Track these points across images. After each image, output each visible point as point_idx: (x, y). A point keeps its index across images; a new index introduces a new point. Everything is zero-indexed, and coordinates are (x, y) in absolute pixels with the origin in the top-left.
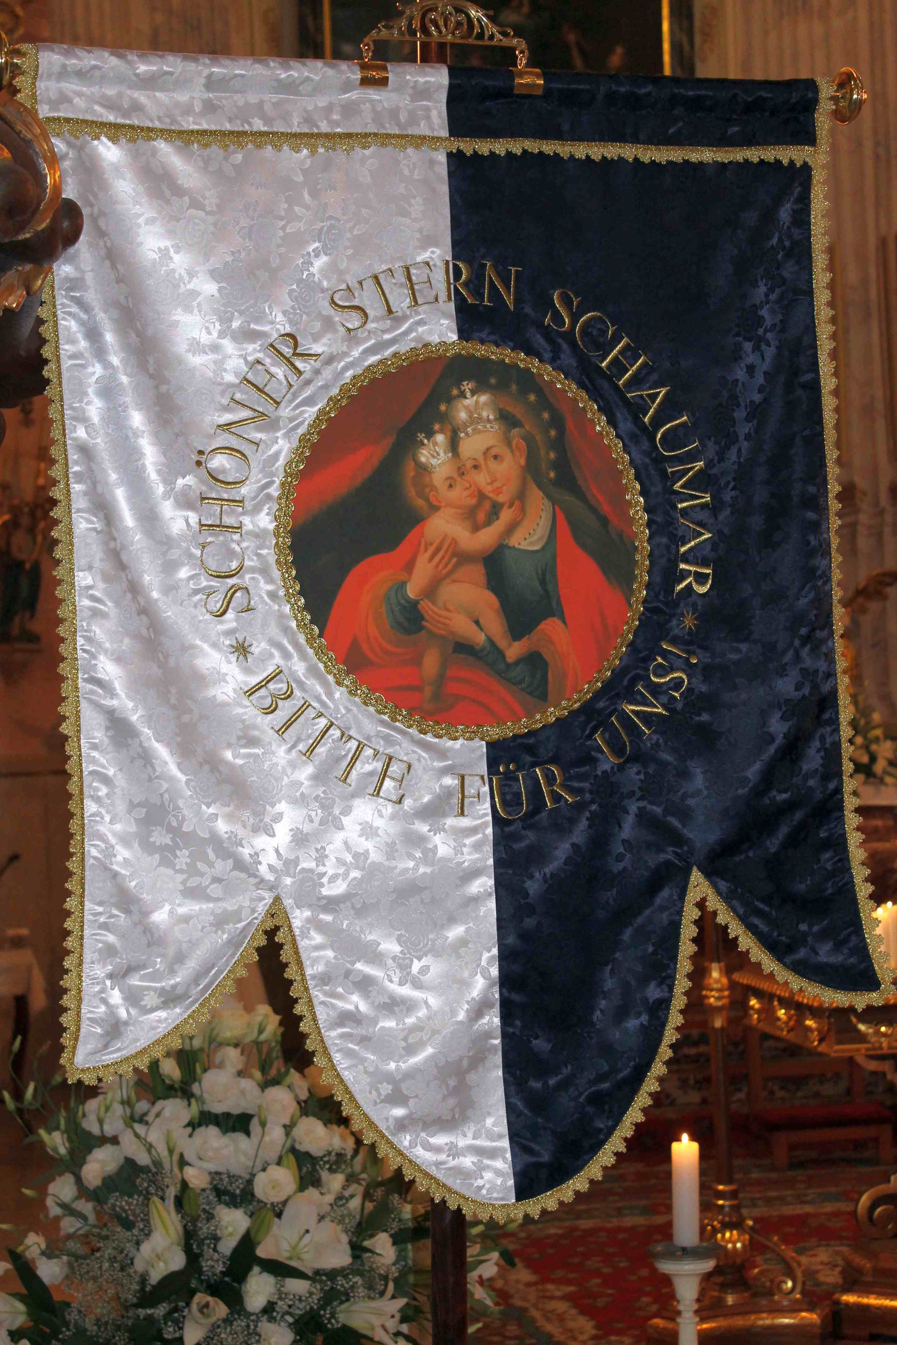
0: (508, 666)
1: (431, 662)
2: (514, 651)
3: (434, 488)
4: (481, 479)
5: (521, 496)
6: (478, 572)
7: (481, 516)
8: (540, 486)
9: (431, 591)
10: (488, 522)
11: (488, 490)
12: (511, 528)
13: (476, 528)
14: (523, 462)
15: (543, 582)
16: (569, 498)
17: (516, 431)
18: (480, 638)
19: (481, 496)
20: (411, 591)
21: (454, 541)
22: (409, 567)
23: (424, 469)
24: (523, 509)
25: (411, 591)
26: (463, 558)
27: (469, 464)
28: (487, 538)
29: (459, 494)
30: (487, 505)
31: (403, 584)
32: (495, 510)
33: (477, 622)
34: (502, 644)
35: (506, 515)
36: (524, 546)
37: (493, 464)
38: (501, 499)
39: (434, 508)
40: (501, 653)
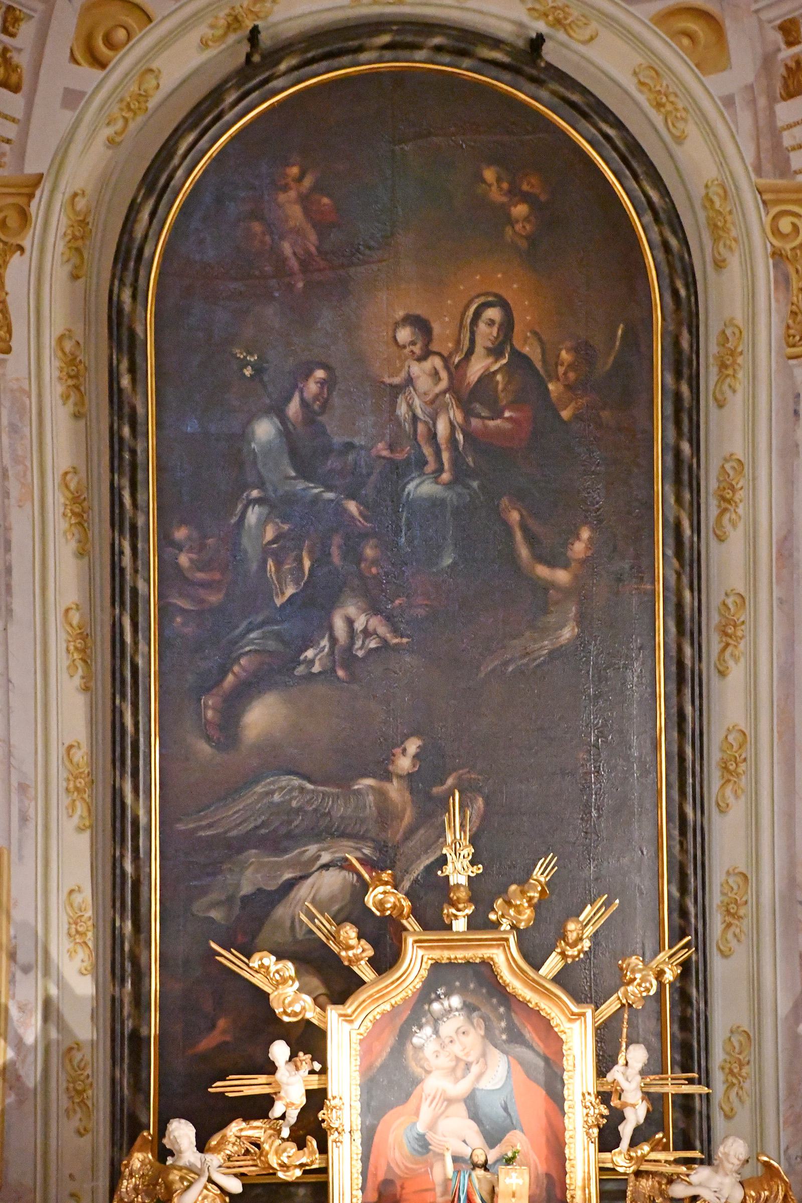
28: (462, 1088)
29: (445, 1061)
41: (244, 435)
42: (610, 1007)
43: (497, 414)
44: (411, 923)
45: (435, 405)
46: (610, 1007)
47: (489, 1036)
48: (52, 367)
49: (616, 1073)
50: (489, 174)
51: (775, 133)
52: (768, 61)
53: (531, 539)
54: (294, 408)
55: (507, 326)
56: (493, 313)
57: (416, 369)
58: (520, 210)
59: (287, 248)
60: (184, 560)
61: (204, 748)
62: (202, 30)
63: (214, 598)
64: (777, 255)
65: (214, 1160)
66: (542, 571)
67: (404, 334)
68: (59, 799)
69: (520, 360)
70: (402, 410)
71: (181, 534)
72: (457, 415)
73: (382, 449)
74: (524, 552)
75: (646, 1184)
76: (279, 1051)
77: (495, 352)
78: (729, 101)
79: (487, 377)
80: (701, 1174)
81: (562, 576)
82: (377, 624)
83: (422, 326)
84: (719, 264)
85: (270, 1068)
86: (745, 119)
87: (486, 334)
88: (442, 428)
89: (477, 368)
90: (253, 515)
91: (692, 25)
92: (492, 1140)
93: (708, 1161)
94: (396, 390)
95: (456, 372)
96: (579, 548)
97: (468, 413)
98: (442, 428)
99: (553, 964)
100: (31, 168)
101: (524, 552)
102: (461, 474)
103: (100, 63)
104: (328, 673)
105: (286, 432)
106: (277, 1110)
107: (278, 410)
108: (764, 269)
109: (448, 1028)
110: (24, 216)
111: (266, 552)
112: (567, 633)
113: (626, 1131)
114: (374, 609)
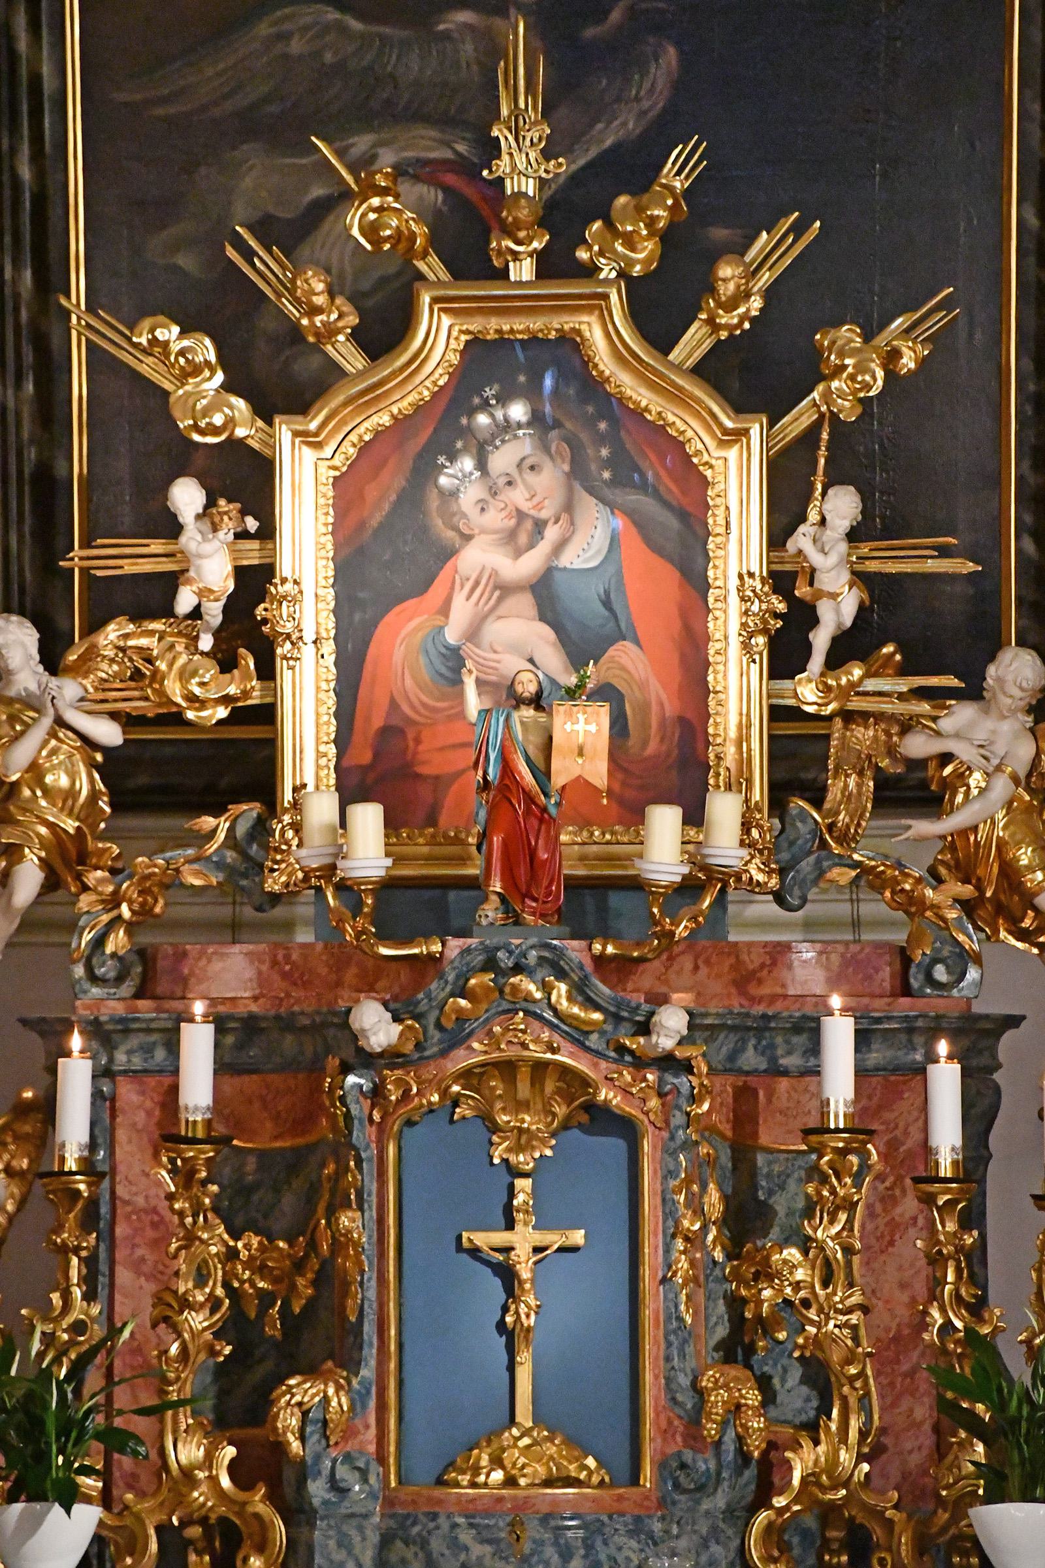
3: (464, 515)
4: (518, 497)
5: (569, 507)
6: (525, 603)
7: (523, 539)
8: (591, 491)
9: (473, 634)
10: (531, 546)
11: (525, 506)
12: (559, 547)
13: (518, 553)
14: (566, 467)
15: (607, 603)
16: (634, 498)
17: (554, 434)
19: (521, 515)
21: (494, 573)
22: (445, 610)
25: (452, 636)
26: (505, 590)
27: (502, 481)
28: (530, 564)
29: (496, 518)
30: (528, 525)
31: (441, 629)
32: (540, 527)
35: (552, 533)
36: (578, 564)
38: (544, 514)
39: (467, 538)
44: (432, 267)
47: (578, 473)
49: (802, 540)
65: (69, 689)
75: (863, 735)
80: (961, 715)
85: (172, 528)
92: (578, 657)
93: (974, 692)
106: (185, 601)
109: (502, 459)
113: (821, 639)
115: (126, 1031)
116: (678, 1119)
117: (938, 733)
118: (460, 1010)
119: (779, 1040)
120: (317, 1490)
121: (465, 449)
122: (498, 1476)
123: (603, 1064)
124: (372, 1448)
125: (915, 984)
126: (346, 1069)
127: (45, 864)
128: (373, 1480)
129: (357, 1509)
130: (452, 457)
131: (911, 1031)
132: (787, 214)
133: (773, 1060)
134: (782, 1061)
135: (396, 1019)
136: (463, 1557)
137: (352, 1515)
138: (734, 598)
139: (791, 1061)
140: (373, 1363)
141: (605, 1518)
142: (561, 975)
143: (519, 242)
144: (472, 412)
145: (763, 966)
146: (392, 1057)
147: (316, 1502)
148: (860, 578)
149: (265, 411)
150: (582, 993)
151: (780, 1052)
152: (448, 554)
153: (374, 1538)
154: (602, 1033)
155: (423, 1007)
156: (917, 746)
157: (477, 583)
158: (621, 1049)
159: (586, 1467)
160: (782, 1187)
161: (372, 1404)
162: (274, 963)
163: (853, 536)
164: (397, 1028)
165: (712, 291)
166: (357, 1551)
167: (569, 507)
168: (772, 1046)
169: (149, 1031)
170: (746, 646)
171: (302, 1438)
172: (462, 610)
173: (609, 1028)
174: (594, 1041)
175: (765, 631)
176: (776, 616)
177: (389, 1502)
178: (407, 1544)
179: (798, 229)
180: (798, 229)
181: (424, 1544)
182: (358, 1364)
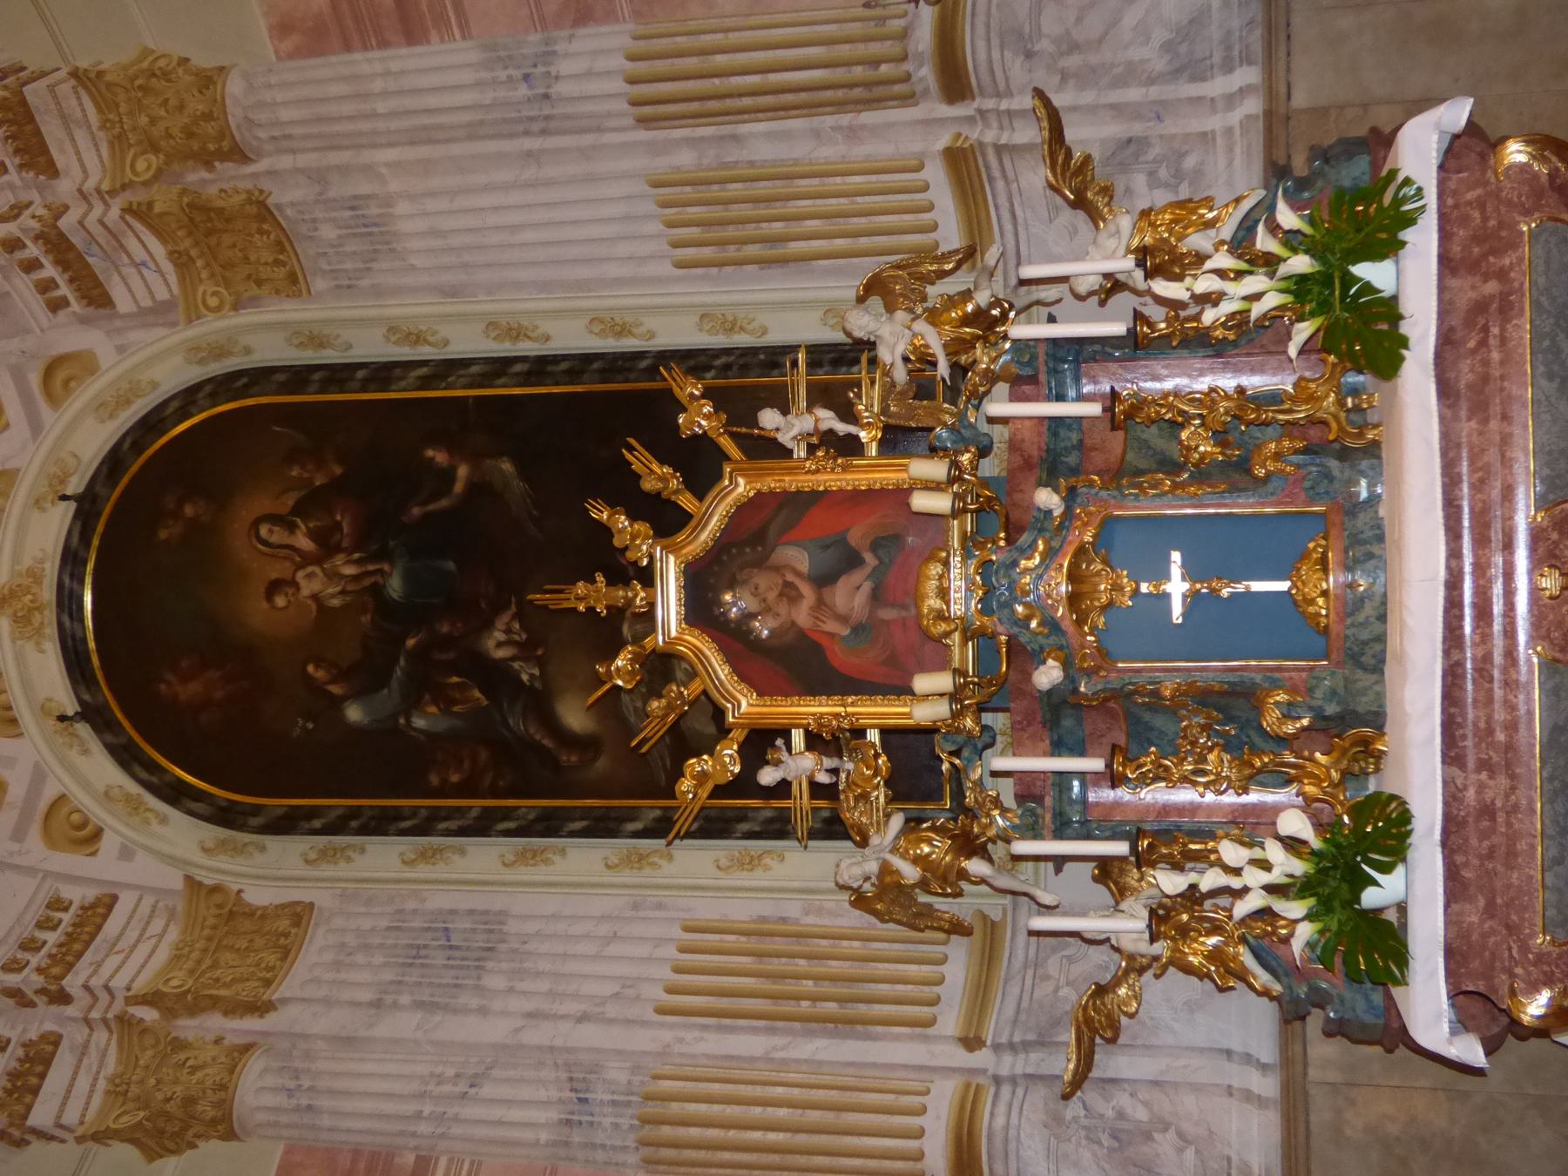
0: (881, 562)
1: (887, 614)
2: (870, 559)
3: (781, 625)
4: (772, 596)
5: (777, 569)
6: (826, 592)
8: (768, 557)
9: (843, 619)
10: (796, 588)
12: (798, 574)
13: (800, 596)
14: (756, 571)
15: (828, 547)
17: (738, 577)
18: (867, 587)
19: (781, 595)
20: (846, 632)
21: (812, 609)
22: (831, 635)
23: (772, 632)
24: (786, 566)
25: (846, 632)
26: (820, 604)
27: (763, 605)
28: (807, 590)
29: (783, 609)
31: (843, 638)
32: (788, 584)
33: (858, 588)
34: (868, 570)
35: (790, 577)
37: (761, 590)
38: (780, 581)
39: (793, 623)
40: (874, 569)
41: (356, 730)
42: (727, 443)
43: (338, 526)
45: (333, 576)
46: (727, 443)
47: (760, 563)
48: (327, 871)
50: (163, 534)
51: (142, 312)
52: (83, 321)
53: (435, 496)
54: (336, 689)
55: (275, 519)
56: (264, 530)
57: (306, 591)
58: (189, 510)
59: (219, 694)
60: (455, 778)
61: (602, 764)
62: (74, 755)
63: (484, 755)
64: (236, 307)
66: (459, 487)
67: (280, 601)
68: (646, 875)
69: (300, 510)
70: (336, 602)
71: (434, 780)
72: (339, 560)
73: (366, 619)
74: (444, 503)
76: (768, 776)
77: (292, 528)
78: (121, 349)
79: (313, 535)
80: (884, 354)
81: (463, 471)
82: (502, 621)
83: (274, 587)
84: (248, 351)
86: (134, 336)
87: (278, 536)
88: (349, 570)
89: (304, 542)
90: (419, 722)
91: (60, 376)
93: (871, 345)
94: (322, 608)
95: (307, 560)
96: (439, 457)
97: (338, 549)
98: (349, 570)
99: (687, 501)
100: (178, 883)
101: (444, 503)
102: (383, 555)
103: (98, 834)
104: (541, 663)
105: (356, 695)
106: (823, 778)
107: (337, 703)
108: (248, 317)
110: (216, 889)
111: (446, 711)
112: (507, 466)
113: (842, 428)
114: (488, 625)
115: (1061, 814)
116: (1104, 494)
117: (892, 365)
118: (1039, 625)
119: (1062, 445)
120: (1331, 709)
121: (747, 625)
122: (1321, 601)
123: (1070, 538)
124: (1304, 675)
125: (1027, 371)
126: (1075, 691)
127: (969, 857)
128: (1324, 675)
129: (1341, 684)
130: (750, 631)
131: (1056, 371)
132: (623, 456)
133: (1073, 447)
134: (1075, 442)
135: (1044, 662)
136: (1372, 620)
137: (1345, 687)
138: (820, 477)
139: (1075, 437)
140: (1253, 675)
141: (1346, 533)
142: (1015, 564)
143: (636, 596)
144: (728, 621)
145: (1022, 456)
146: (1066, 665)
147: (1338, 709)
148: (809, 409)
149: (724, 731)
150: (1028, 552)
151: (1069, 444)
152: (802, 635)
153: (1360, 674)
154: (1051, 538)
155: (1037, 647)
156: (900, 375)
157: (817, 618)
158: (1061, 527)
159: (1315, 548)
160: (1146, 441)
161: (1277, 675)
162: (1023, 729)
163: (785, 412)
164: (1051, 662)
165: (659, 494)
166: (1367, 684)
167: (777, 569)
168: (1066, 448)
169: (1060, 800)
170: (845, 469)
171: (1299, 718)
172: (831, 626)
173: (1048, 535)
174: (1055, 544)
175: (835, 459)
176: (827, 452)
177: (1339, 664)
178: (1363, 654)
179: (631, 449)
180: (631, 449)
181: (1365, 643)
182: (1254, 684)
